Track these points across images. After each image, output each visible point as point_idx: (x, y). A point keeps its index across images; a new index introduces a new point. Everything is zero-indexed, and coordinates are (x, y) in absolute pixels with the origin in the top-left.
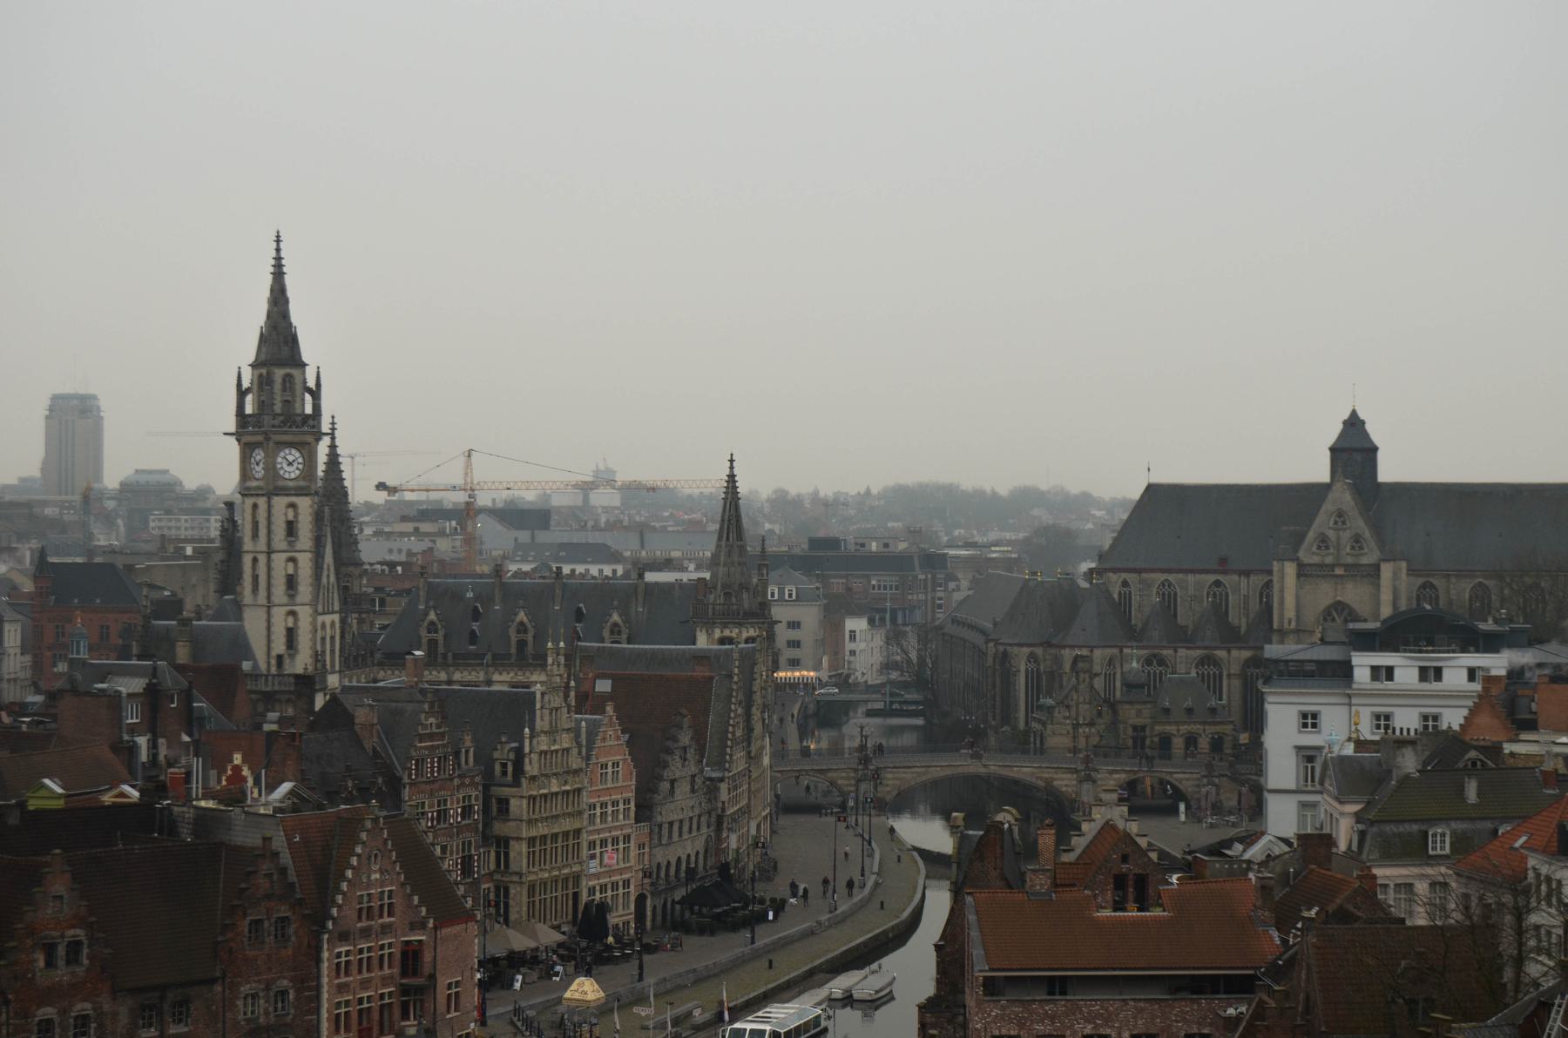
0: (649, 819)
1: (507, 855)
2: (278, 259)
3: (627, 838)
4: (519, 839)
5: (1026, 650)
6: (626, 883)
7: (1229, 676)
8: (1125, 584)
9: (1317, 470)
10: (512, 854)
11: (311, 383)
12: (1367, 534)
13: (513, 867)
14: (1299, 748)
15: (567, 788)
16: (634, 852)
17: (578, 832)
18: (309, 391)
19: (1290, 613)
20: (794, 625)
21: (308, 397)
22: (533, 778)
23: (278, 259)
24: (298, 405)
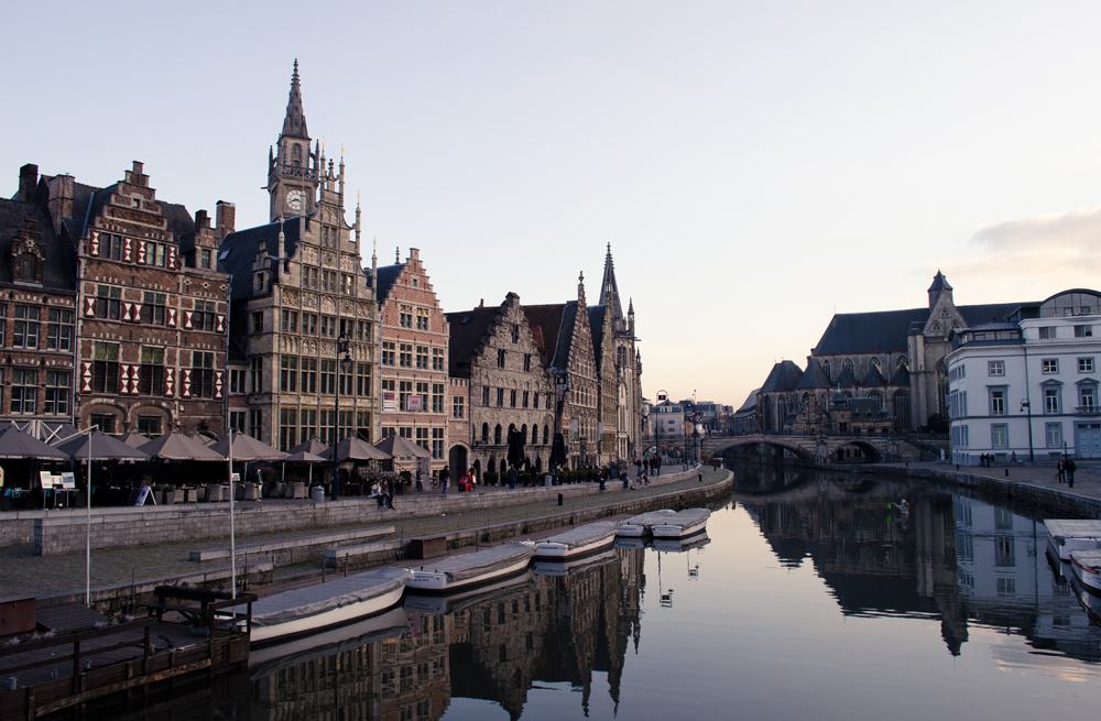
0: (468, 376)
1: (260, 373)
2: (296, 75)
3: (438, 388)
4: (270, 354)
5: (778, 394)
6: (438, 433)
7: (886, 401)
8: (826, 361)
9: (923, 302)
10: (264, 373)
11: (313, 151)
12: (961, 319)
13: (265, 389)
14: (990, 387)
15: (350, 315)
16: (448, 404)
17: (366, 368)
18: (312, 155)
19: (921, 362)
20: (671, 422)
21: (311, 159)
22: (296, 291)
23: (296, 75)
24: (304, 165)
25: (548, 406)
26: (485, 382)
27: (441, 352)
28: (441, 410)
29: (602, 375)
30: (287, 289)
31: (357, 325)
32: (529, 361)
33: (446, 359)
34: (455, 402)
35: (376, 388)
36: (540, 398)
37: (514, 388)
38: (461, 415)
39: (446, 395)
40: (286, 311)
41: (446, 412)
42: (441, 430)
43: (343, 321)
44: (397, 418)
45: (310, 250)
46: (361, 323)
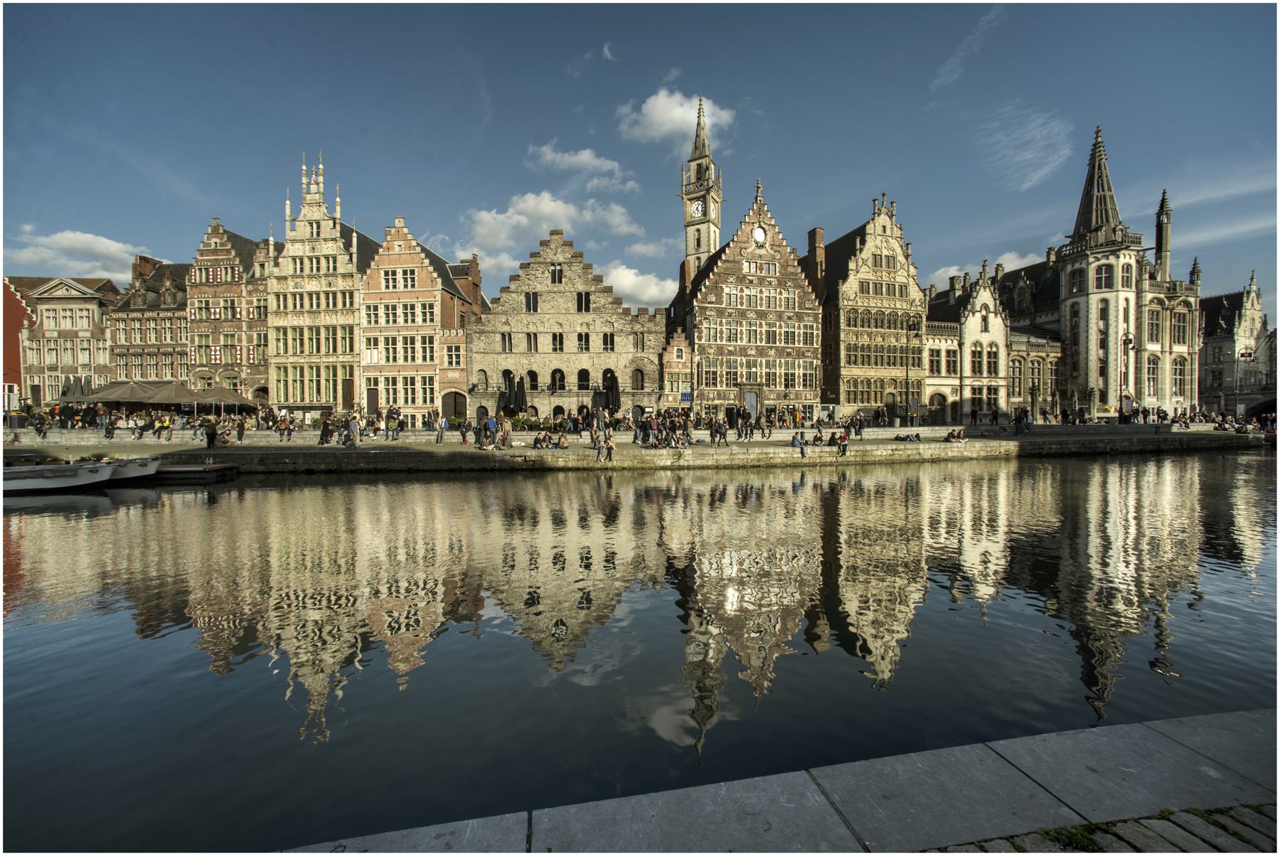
16: (440, 353)
22: (285, 278)
25: (640, 343)
26: (506, 329)
27: (431, 306)
28: (432, 358)
29: (844, 304)
30: (279, 279)
31: (339, 296)
32: (588, 301)
33: (437, 310)
34: (450, 349)
35: (360, 344)
36: (616, 339)
37: (557, 330)
38: (458, 363)
39: (436, 345)
40: (278, 296)
41: (437, 361)
42: (431, 379)
43: (327, 294)
44: (380, 369)
45: (298, 245)
46: (344, 294)
